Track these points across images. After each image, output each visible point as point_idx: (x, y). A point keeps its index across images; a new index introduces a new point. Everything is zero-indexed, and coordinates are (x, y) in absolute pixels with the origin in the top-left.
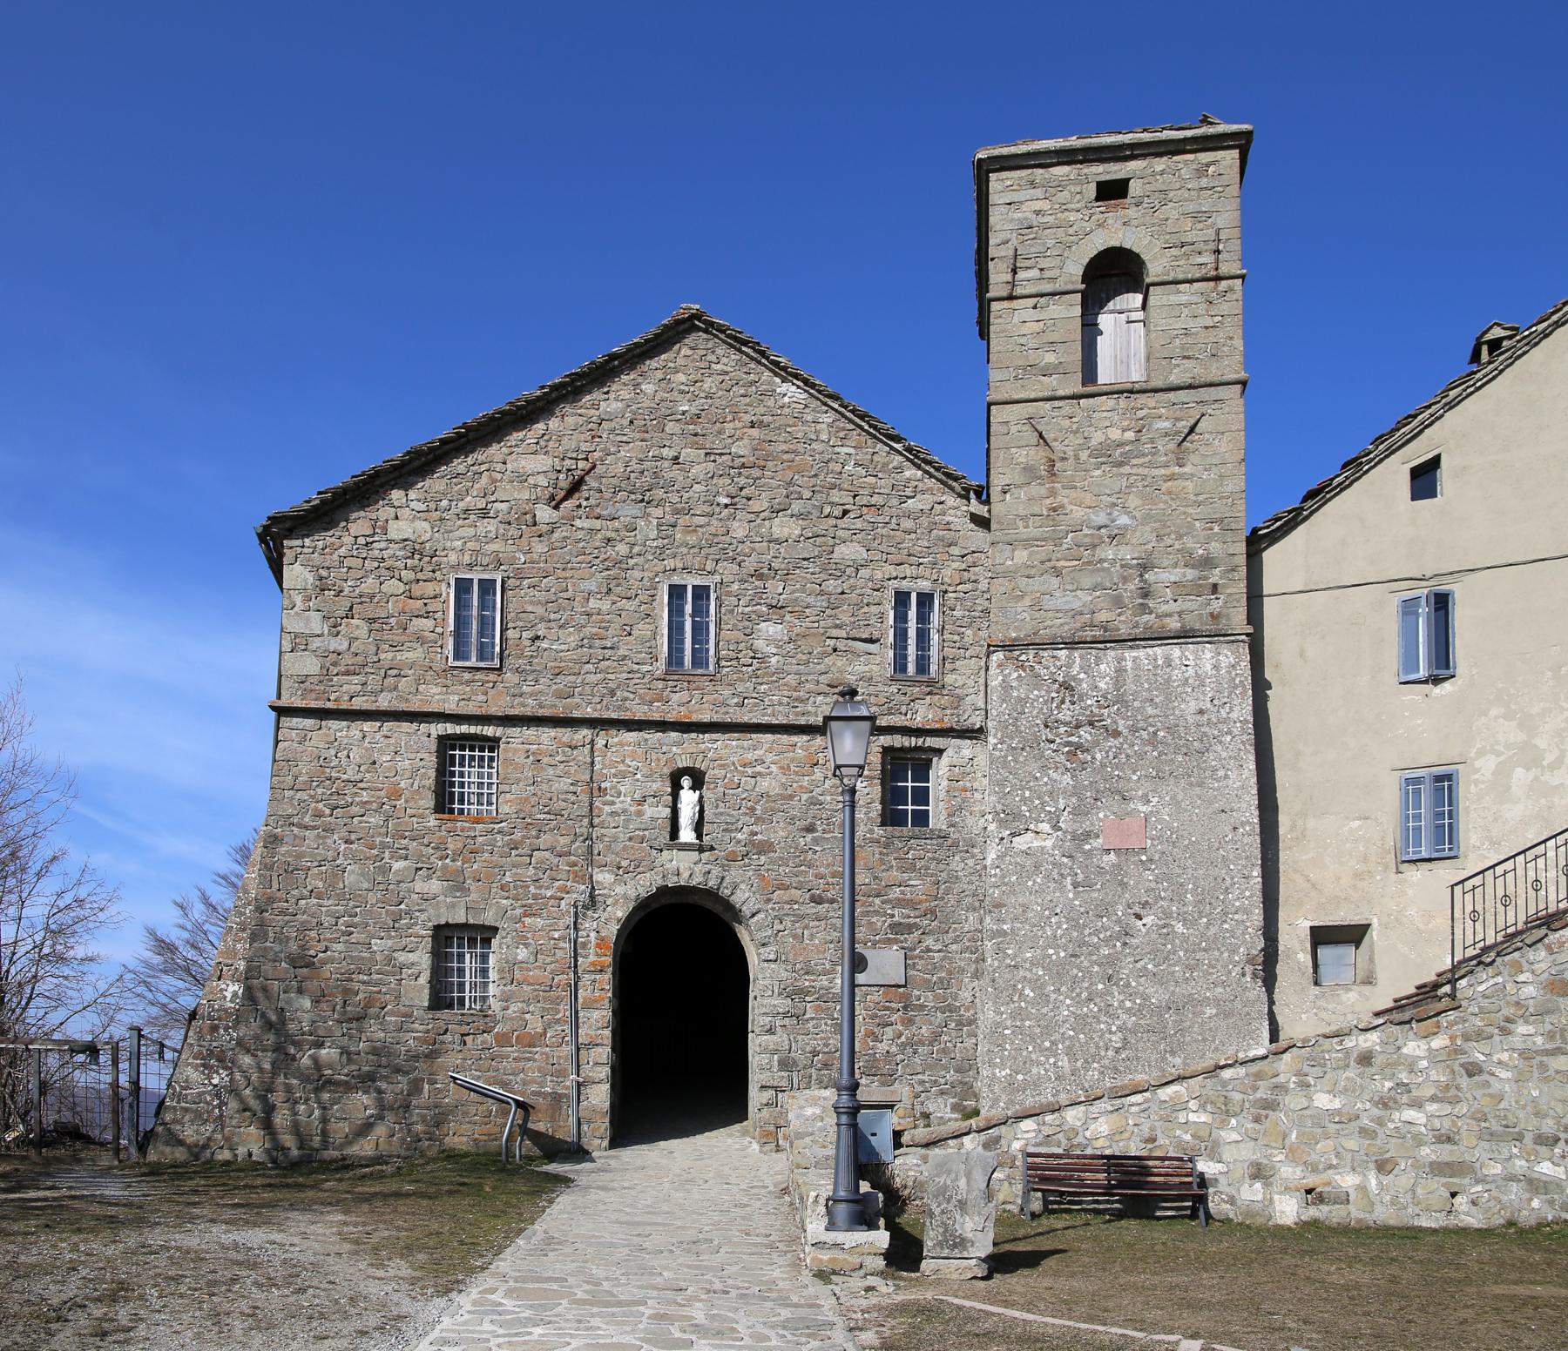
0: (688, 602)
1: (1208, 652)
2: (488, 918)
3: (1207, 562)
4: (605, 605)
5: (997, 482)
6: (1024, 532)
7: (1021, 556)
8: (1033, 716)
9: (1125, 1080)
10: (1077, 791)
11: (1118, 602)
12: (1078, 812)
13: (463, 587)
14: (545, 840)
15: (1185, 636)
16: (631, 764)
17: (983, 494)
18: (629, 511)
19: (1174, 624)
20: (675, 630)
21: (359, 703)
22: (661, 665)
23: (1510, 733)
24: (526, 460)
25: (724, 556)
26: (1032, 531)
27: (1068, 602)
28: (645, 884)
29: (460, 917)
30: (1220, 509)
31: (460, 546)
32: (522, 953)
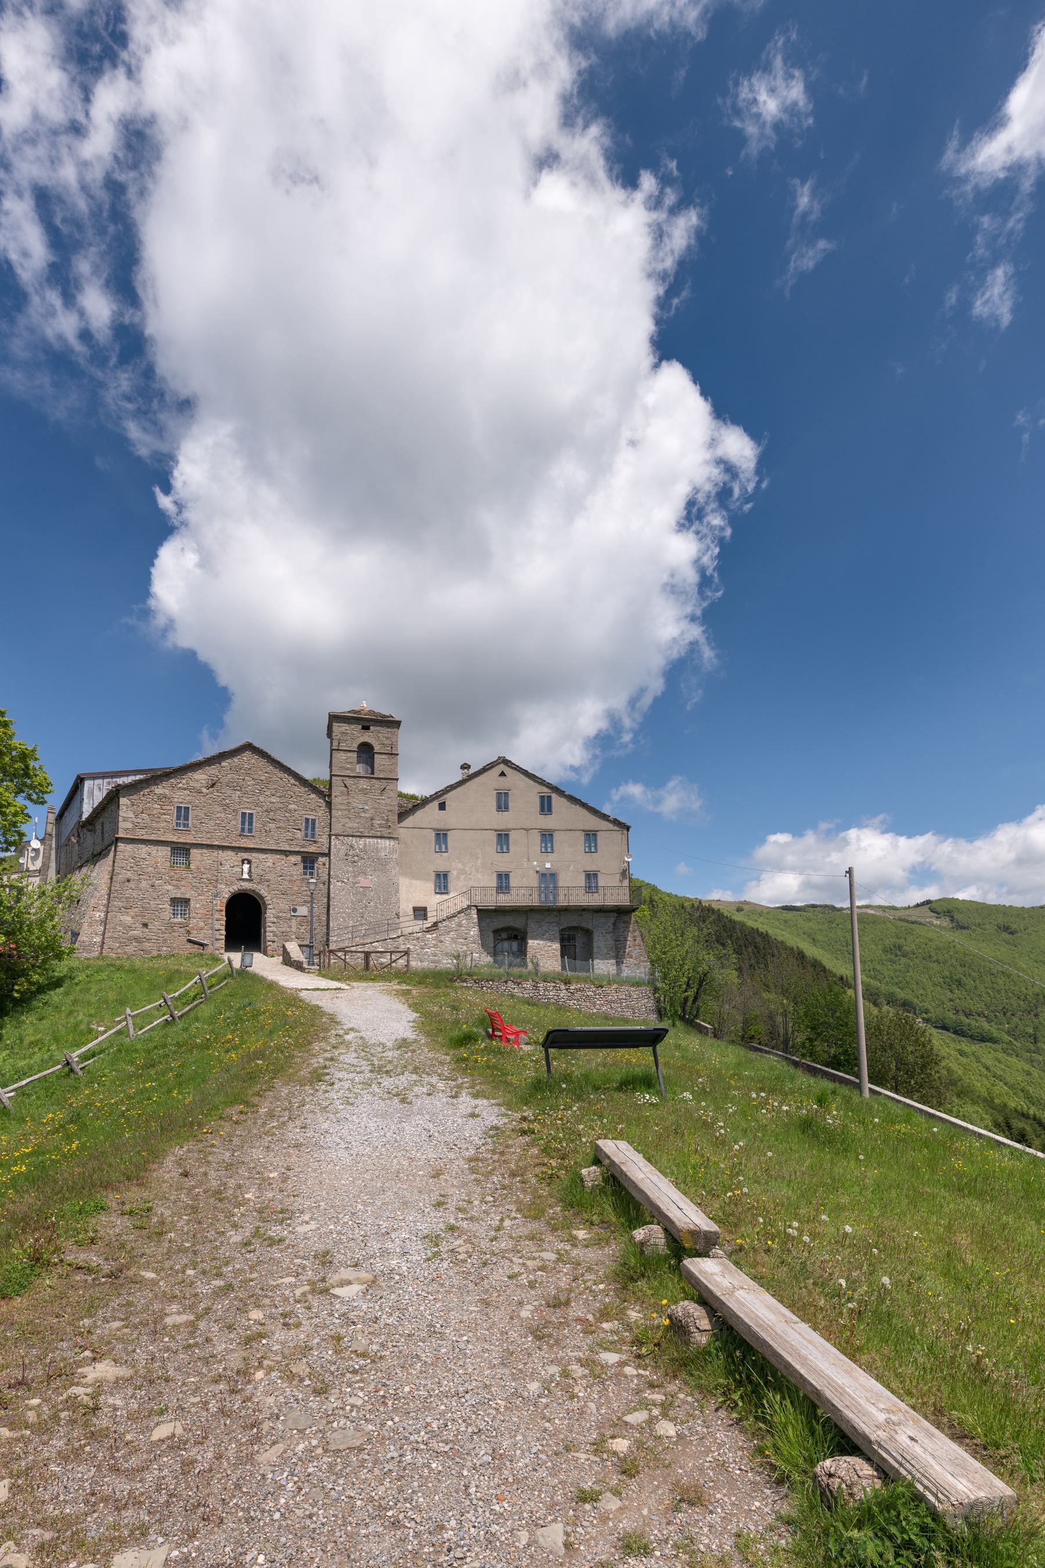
0: (247, 819)
1: (387, 841)
2: (187, 896)
3: (387, 820)
4: (223, 815)
5: (334, 794)
6: (340, 807)
7: (340, 813)
8: (342, 853)
9: (366, 941)
10: (354, 872)
11: (364, 827)
12: (355, 877)
13: (179, 808)
14: (204, 876)
15: (381, 837)
16: (230, 858)
17: (330, 796)
18: (229, 792)
19: (379, 834)
20: (243, 823)
21: (144, 837)
22: (239, 832)
23: (460, 866)
24: (200, 777)
25: (257, 805)
26: (343, 807)
27: (353, 825)
28: (235, 888)
29: (179, 896)
30: (391, 808)
31: (180, 797)
32: (198, 906)
